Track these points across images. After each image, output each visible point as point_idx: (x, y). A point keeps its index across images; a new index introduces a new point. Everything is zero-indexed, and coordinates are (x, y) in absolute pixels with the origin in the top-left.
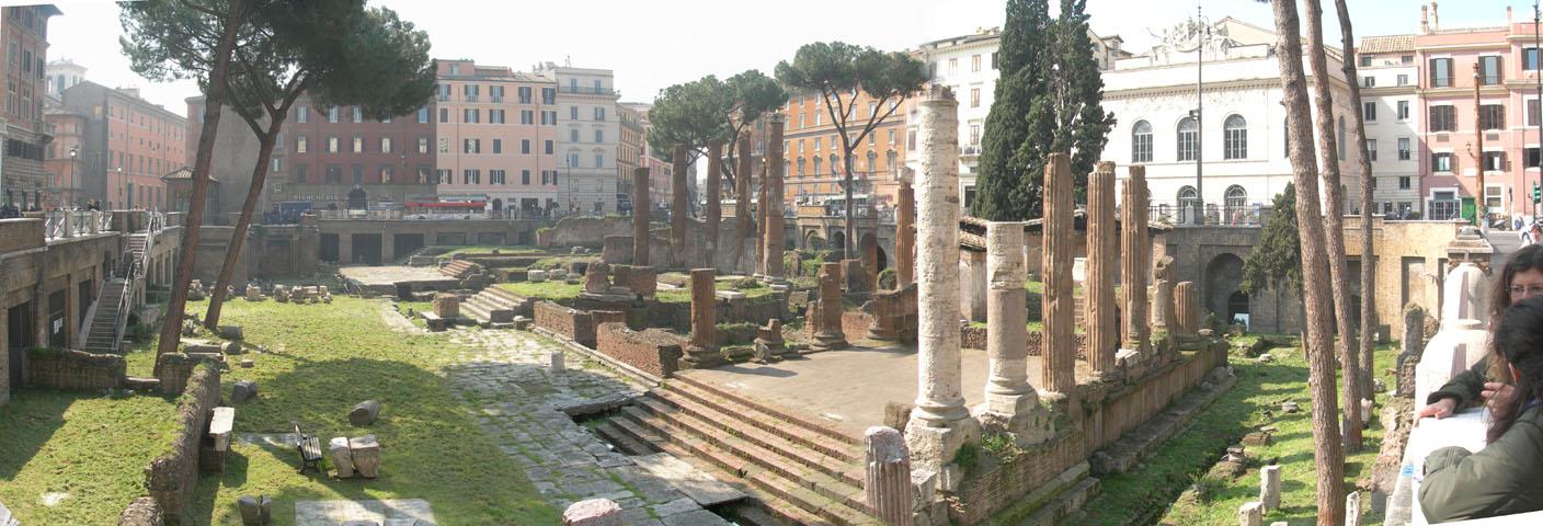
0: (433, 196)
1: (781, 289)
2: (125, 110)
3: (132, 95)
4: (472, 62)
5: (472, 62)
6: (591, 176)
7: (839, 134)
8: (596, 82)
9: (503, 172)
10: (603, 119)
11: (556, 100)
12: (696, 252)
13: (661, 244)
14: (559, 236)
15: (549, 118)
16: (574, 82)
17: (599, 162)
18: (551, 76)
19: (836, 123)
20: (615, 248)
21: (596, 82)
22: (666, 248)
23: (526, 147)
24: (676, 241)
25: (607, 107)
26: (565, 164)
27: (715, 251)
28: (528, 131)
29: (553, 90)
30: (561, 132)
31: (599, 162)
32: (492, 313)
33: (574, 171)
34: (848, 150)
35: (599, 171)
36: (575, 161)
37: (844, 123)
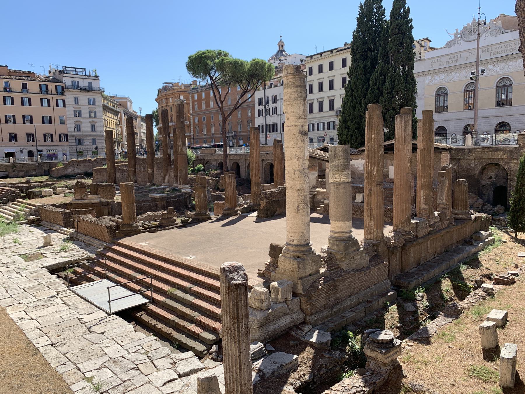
4: (6, 66)
5: (6, 66)
6: (90, 136)
8: (89, 83)
10: (94, 104)
11: (65, 93)
15: (60, 103)
17: (93, 128)
21: (89, 83)
22: (126, 173)
26: (72, 129)
29: (62, 87)
30: (69, 111)
31: (93, 128)
32: (14, 216)
33: (78, 134)
36: (78, 128)
37: (222, 105)
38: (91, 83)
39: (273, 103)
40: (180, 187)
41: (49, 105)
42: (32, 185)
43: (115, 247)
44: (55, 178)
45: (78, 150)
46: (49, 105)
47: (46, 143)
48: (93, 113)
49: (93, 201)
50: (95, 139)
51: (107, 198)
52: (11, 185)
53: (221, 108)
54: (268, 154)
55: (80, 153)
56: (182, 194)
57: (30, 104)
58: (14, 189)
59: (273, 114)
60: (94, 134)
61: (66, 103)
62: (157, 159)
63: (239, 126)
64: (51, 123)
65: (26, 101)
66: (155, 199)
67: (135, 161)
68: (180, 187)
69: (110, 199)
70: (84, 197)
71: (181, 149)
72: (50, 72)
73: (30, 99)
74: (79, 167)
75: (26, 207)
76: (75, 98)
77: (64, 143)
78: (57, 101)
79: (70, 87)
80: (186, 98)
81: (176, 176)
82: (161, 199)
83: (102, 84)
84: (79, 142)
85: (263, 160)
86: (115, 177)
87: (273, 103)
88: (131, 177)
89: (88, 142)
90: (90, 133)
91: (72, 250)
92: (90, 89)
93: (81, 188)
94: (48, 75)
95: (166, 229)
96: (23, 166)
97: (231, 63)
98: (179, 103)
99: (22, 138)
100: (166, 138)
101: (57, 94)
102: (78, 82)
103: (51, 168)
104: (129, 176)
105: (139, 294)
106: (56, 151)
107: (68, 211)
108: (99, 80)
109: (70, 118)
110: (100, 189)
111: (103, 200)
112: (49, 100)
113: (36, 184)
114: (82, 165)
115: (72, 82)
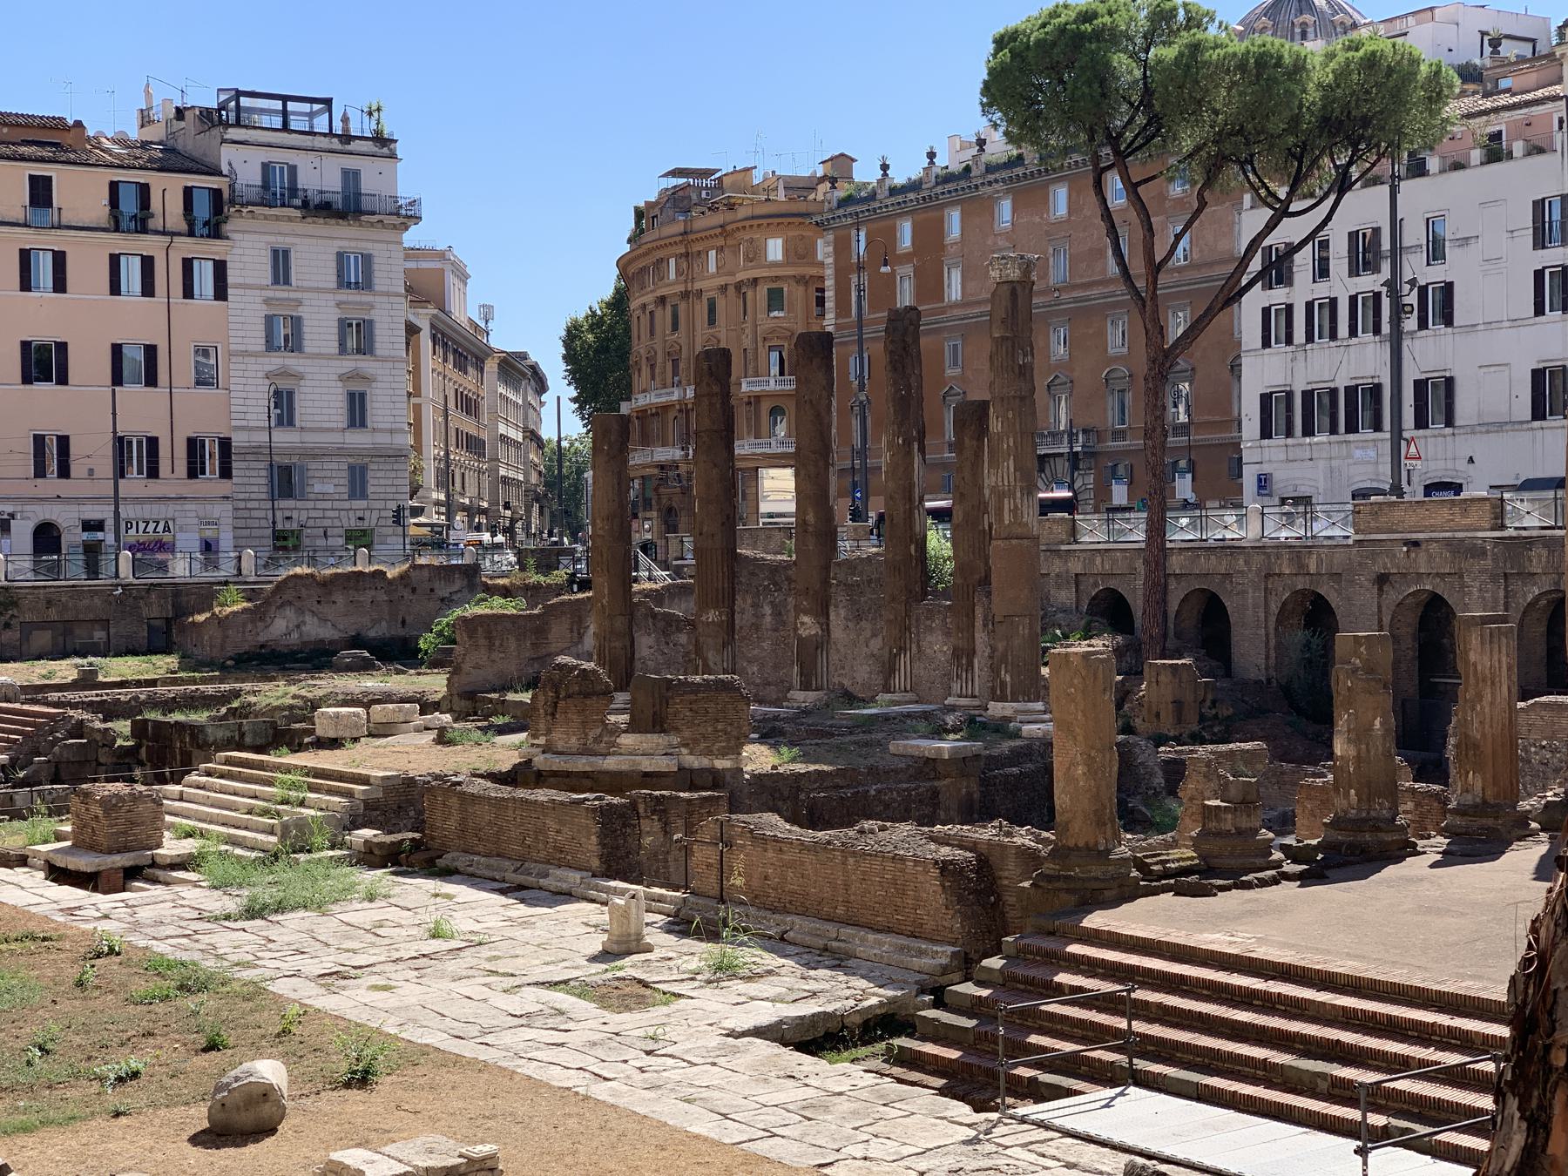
6: (340, 452)
8: (346, 173)
10: (366, 284)
11: (227, 228)
13: (670, 625)
21: (346, 173)
22: (683, 638)
25: (378, 251)
27: (822, 643)
28: (135, 319)
29: (216, 194)
30: (244, 318)
35: (357, 439)
36: (283, 404)
38: (357, 173)
39: (1354, 272)
40: (997, 709)
43: (1075, 949)
44: (210, 664)
45: (279, 527)
46: (148, 289)
47: (199, 486)
48: (357, 336)
49: (647, 765)
50: (364, 469)
51: (708, 752)
52: (34, 692)
53: (1148, 305)
54: (1416, 544)
55: (284, 542)
56: (1029, 747)
57: (60, 285)
58: (77, 714)
59: (1353, 332)
60: (357, 439)
61: (232, 277)
62: (851, 565)
63: (1112, 402)
64: (151, 381)
65: (44, 270)
66: (929, 767)
67: (732, 576)
68: (997, 709)
69: (723, 754)
70: (597, 740)
71: (1015, 511)
72: (145, 120)
73: (59, 259)
74: (325, 609)
75: (313, 788)
76: (275, 252)
77: (210, 483)
78: (188, 264)
79: (253, 194)
80: (799, 253)
81: (963, 656)
82: (961, 763)
83: (407, 180)
84: (285, 481)
85: (1382, 580)
86: (631, 659)
87: (1354, 272)
89: (327, 483)
90: (336, 438)
91: (770, 972)
92: (346, 207)
93: (587, 696)
94: (134, 134)
95: (1248, 886)
96: (49, 603)
97: (1242, 66)
98: (1014, 274)
99: (93, 451)
100: (909, 453)
101: (191, 234)
102: (293, 170)
103: (181, 611)
104: (698, 649)
105: (1394, 1145)
106: (167, 529)
107: (616, 800)
108: (393, 156)
109: (246, 354)
110: (678, 707)
111: (694, 761)
112: (148, 264)
113: (143, 693)
114: (339, 598)
115: (266, 168)
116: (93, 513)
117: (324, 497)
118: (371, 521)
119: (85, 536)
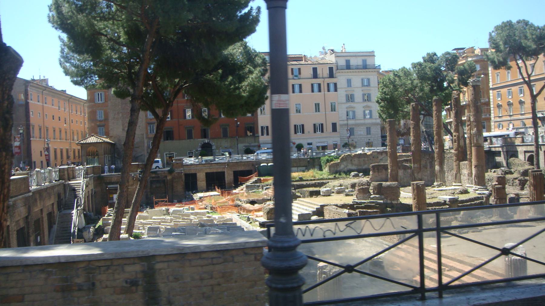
0: (257, 144)
1: (484, 194)
2: (40, 95)
3: (44, 84)
7: (525, 87)
9: (303, 126)
10: (369, 85)
12: (429, 172)
13: (405, 168)
14: (342, 166)
15: (332, 87)
16: (348, 62)
18: (331, 59)
19: (523, 78)
20: (378, 172)
23: (317, 106)
24: (416, 165)
26: (345, 117)
28: (318, 97)
33: (351, 122)
34: (534, 98)
41: (320, 91)
42: (304, 183)
46: (320, 91)
50: (370, 128)
57: (301, 91)
61: (338, 86)
76: (348, 80)
78: (328, 84)
88: (416, 175)
108: (374, 56)
109: (342, 103)
112: (319, 85)
116: (310, 141)
117: (361, 135)
118: (372, 140)
119: (308, 146)
